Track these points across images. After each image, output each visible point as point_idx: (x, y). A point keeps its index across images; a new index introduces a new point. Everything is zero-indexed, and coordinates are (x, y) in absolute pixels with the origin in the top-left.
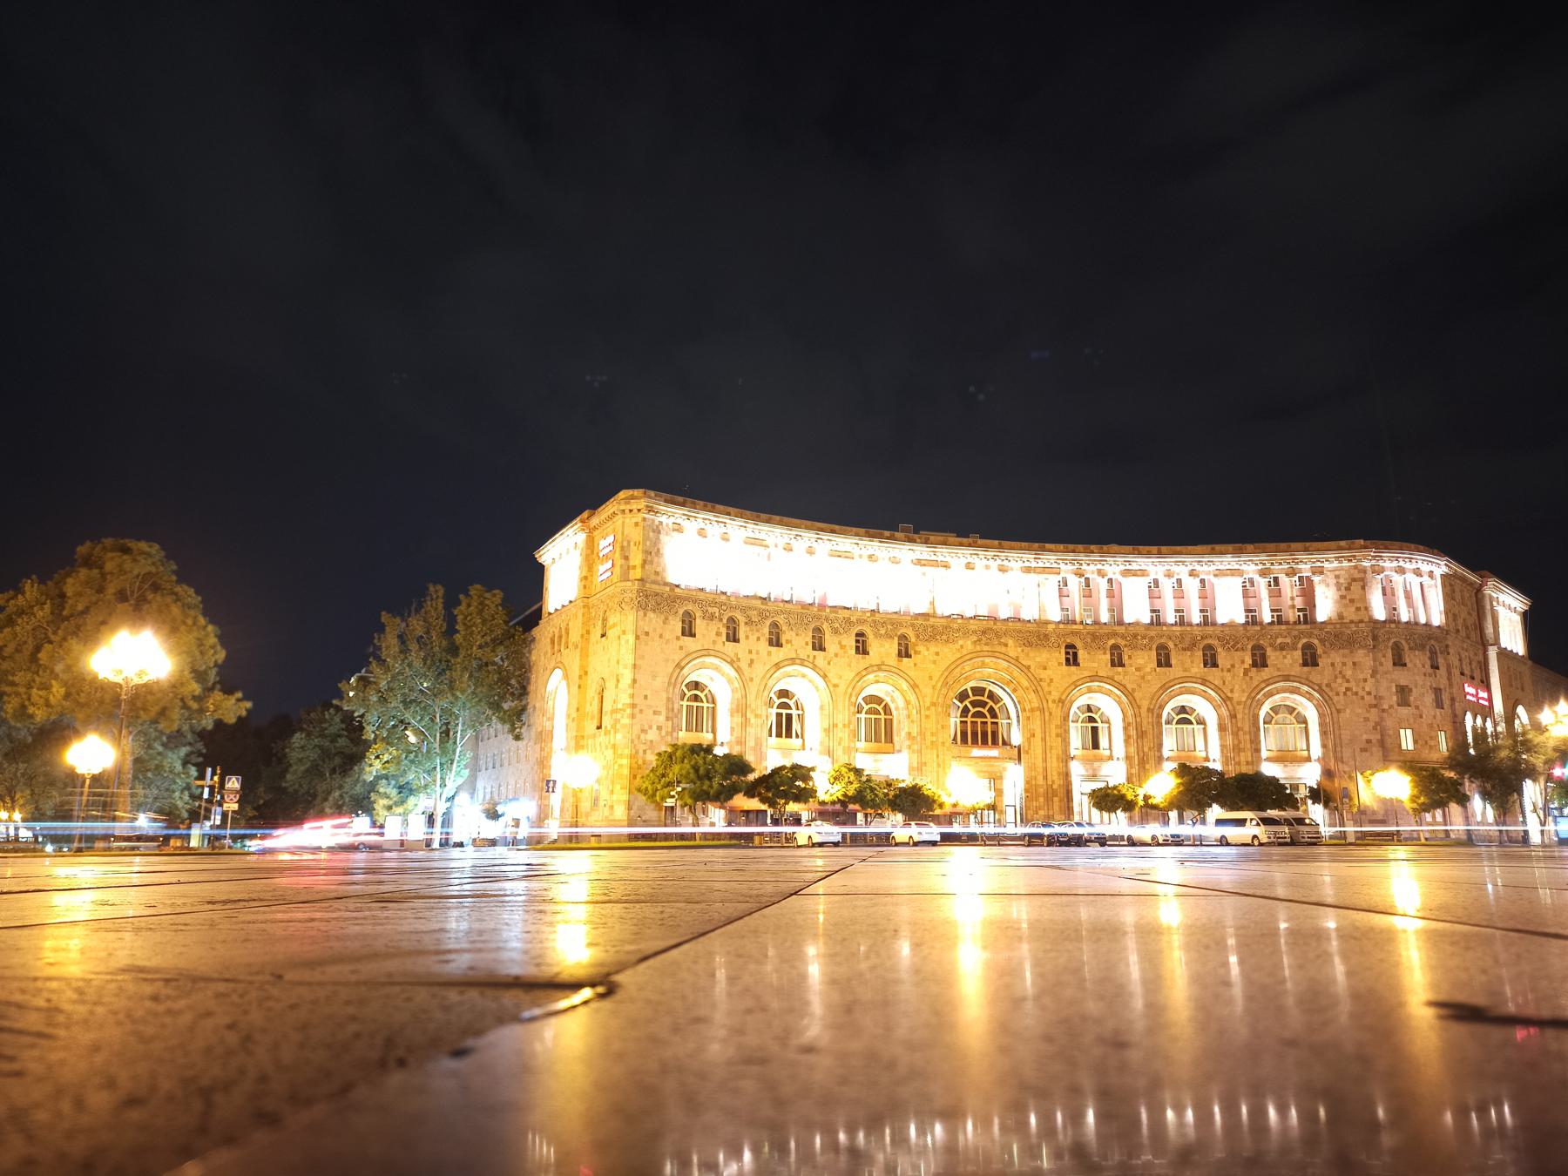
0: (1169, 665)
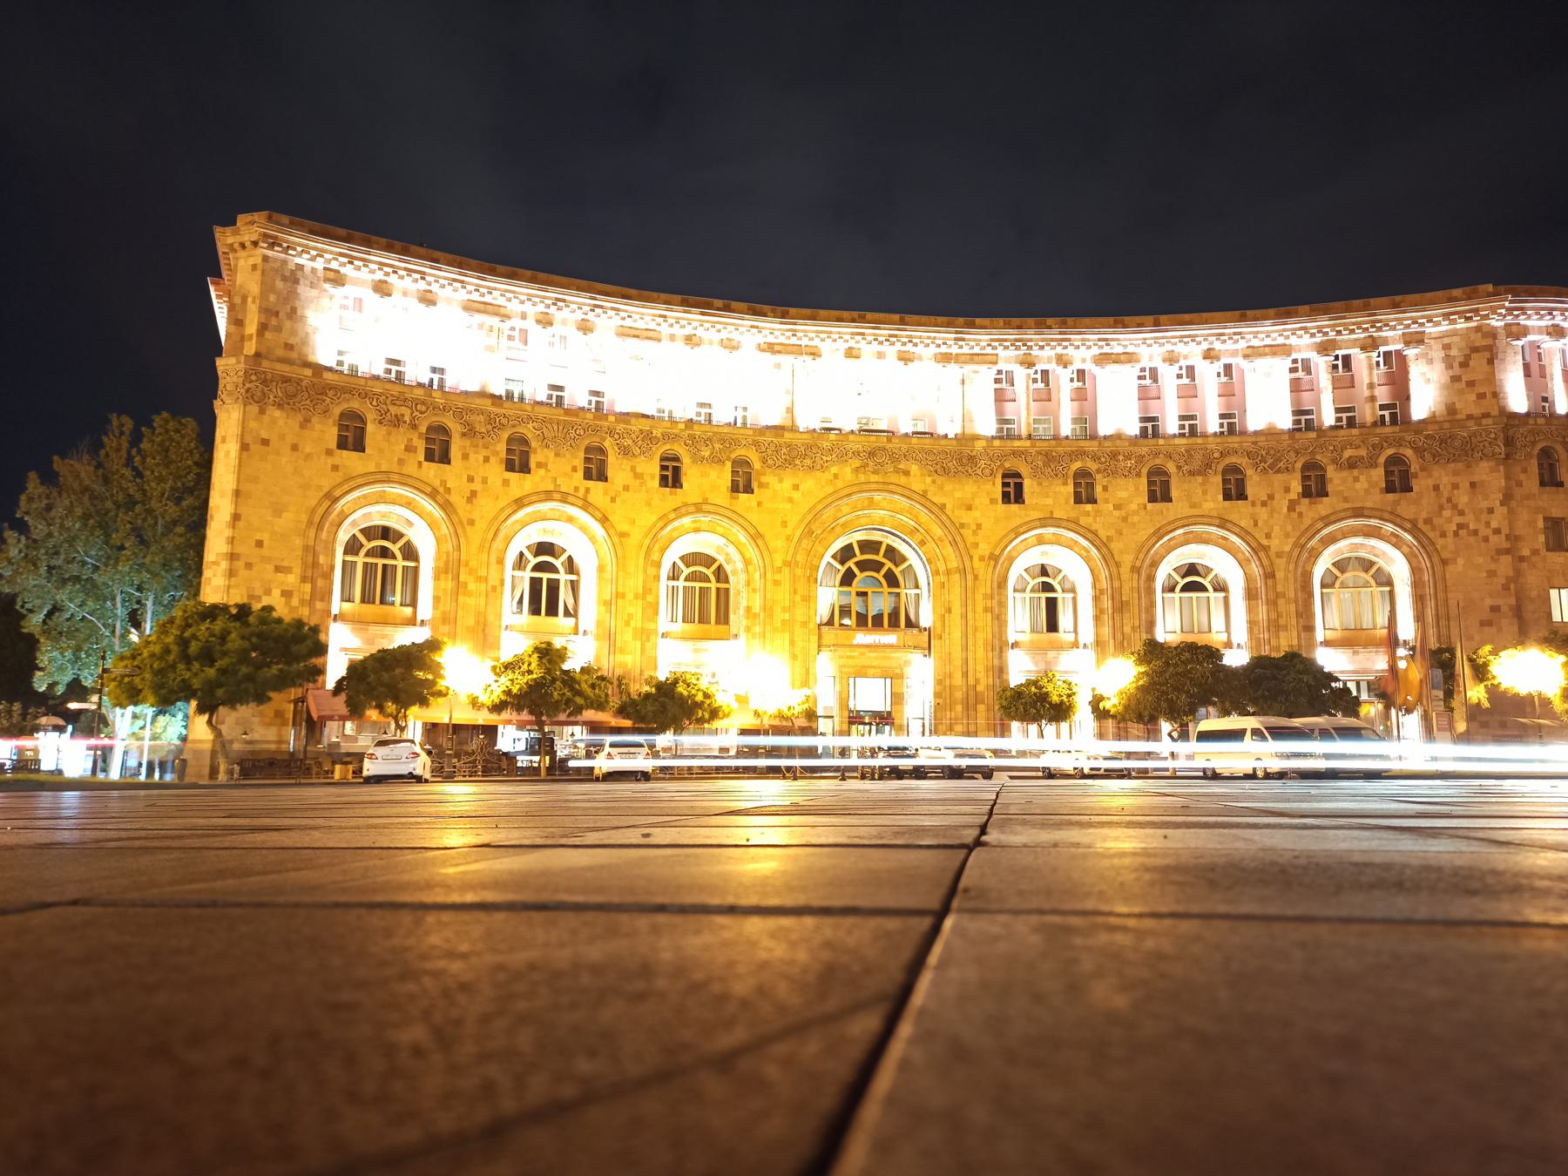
0: (1167, 498)
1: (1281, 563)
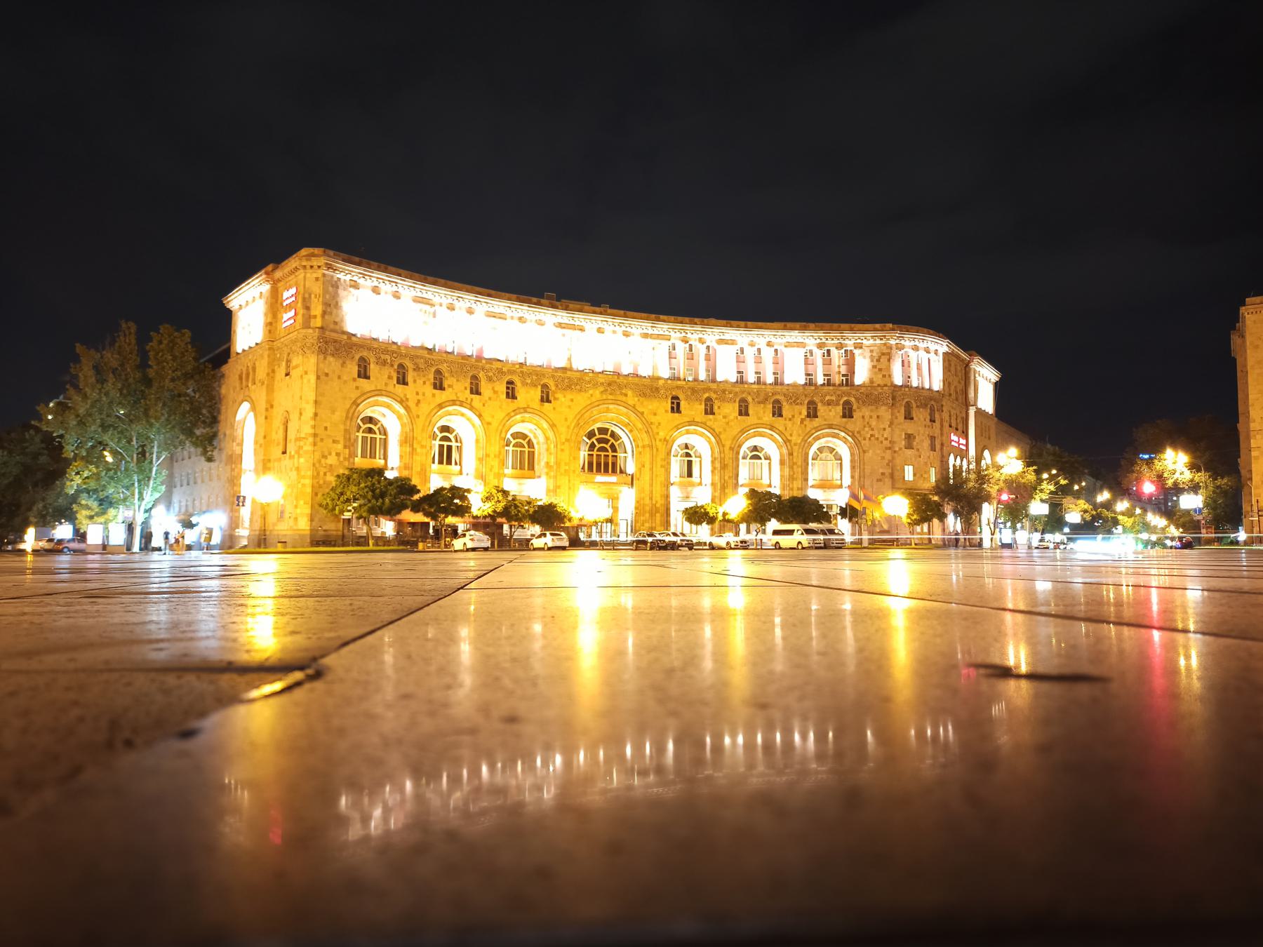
0: (747, 414)
1: (796, 448)
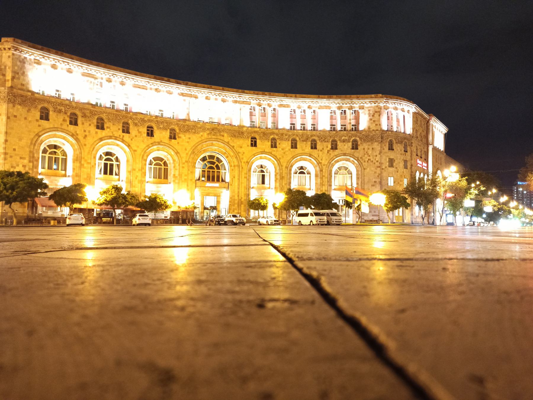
0: (296, 148)
1: (324, 167)
